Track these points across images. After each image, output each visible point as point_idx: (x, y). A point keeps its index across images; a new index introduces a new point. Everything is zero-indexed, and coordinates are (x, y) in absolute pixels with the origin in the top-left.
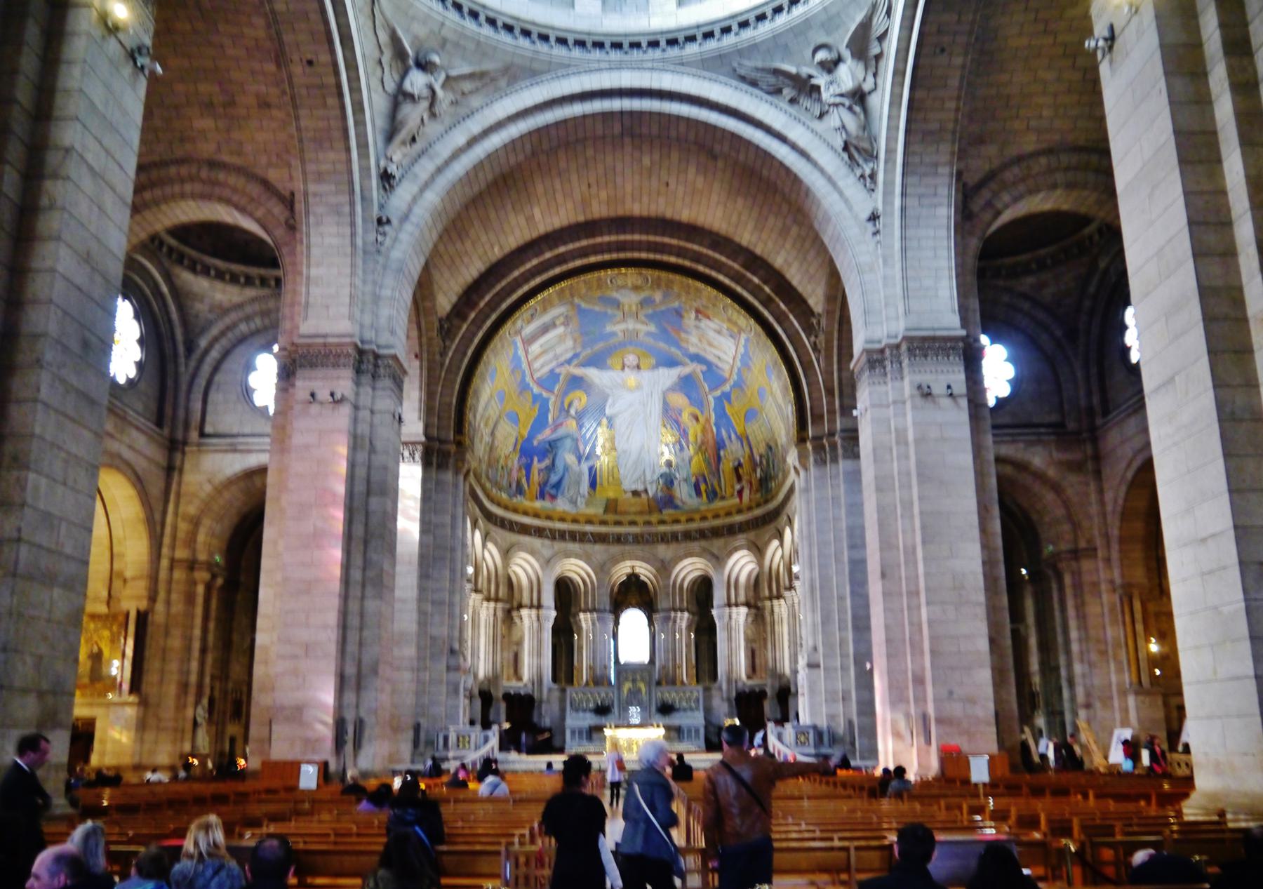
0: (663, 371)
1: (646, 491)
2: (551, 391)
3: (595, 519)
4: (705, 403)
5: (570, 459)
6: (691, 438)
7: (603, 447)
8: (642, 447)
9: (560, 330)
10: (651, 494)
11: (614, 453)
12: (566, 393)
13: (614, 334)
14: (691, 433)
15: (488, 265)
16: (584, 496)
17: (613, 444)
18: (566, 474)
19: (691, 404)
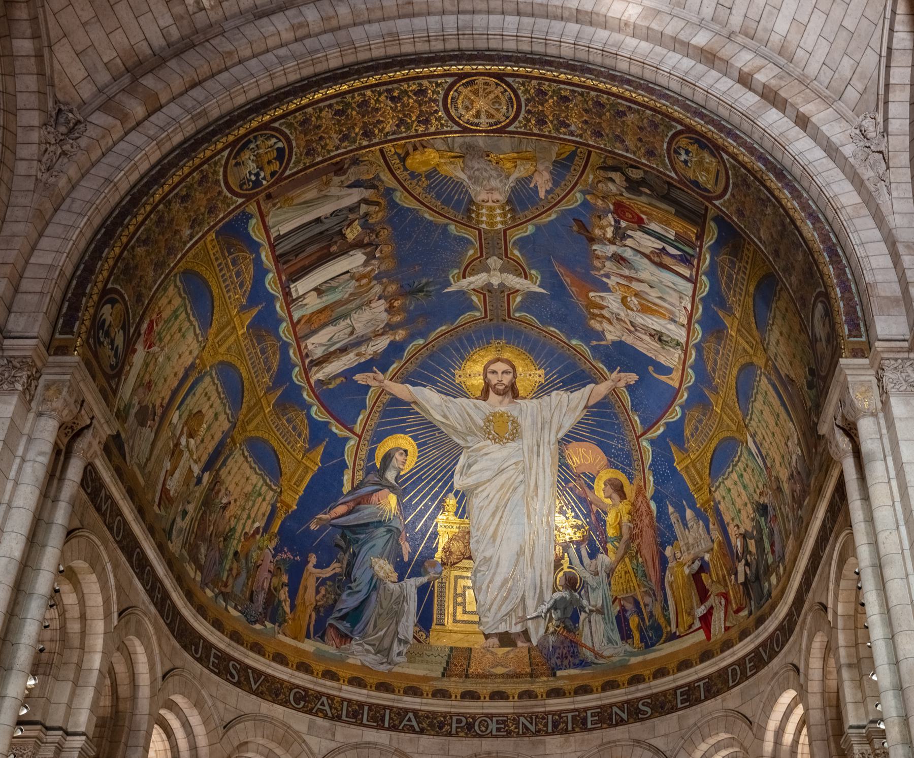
0: (558, 397)
1: (525, 634)
2: (348, 425)
3: (425, 687)
4: (636, 455)
5: (384, 568)
6: (611, 532)
7: (447, 550)
8: (520, 553)
9: (355, 260)
10: (535, 643)
11: (466, 563)
12: (379, 437)
13: (462, 302)
14: (610, 518)
15: (187, 31)
16: (406, 642)
17: (467, 545)
18: (374, 597)
19: (611, 465)
